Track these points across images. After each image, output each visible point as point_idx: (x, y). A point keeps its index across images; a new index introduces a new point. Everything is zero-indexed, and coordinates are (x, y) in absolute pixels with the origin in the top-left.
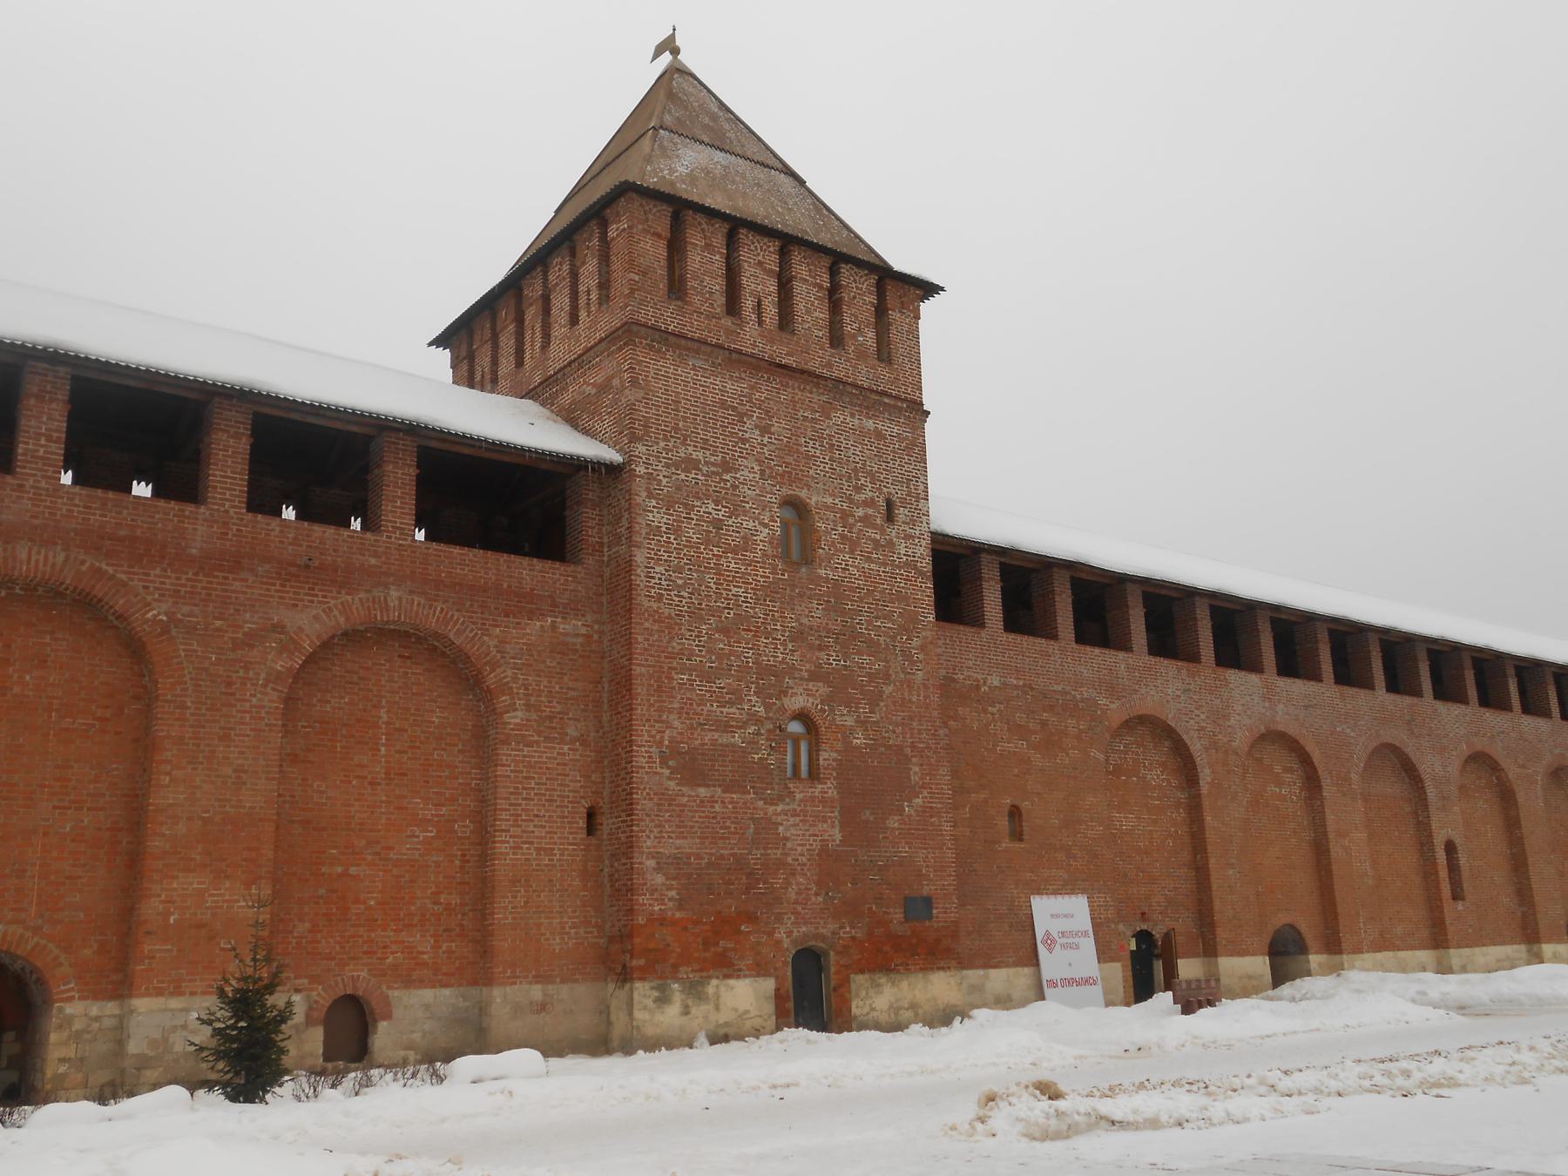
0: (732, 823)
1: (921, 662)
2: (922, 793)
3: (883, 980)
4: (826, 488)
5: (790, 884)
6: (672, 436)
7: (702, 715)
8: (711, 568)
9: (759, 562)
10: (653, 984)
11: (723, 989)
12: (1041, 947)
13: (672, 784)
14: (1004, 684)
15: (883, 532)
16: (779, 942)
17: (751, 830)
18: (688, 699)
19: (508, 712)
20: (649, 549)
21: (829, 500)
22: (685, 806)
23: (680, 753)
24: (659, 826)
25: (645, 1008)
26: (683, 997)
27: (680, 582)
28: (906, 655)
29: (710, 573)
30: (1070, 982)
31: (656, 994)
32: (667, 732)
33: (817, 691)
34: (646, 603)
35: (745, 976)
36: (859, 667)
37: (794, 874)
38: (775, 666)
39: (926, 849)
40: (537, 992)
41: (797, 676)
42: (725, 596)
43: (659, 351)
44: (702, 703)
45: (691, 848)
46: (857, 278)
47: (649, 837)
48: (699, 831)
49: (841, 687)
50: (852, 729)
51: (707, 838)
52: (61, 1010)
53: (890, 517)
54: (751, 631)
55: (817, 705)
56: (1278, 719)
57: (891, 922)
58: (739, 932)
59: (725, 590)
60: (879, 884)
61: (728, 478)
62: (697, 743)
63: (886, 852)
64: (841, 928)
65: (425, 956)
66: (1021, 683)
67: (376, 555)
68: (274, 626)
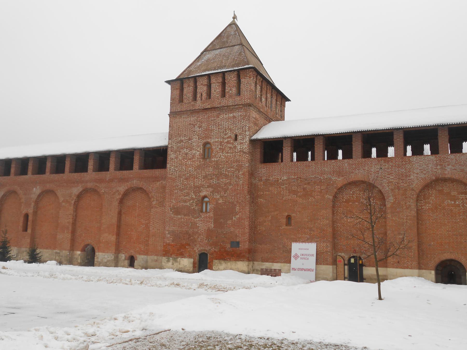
0: (186, 223)
1: (242, 178)
2: (239, 214)
3: (223, 262)
4: (216, 137)
5: (199, 237)
6: (177, 136)
7: (180, 199)
8: (184, 165)
9: (196, 161)
10: (167, 258)
11: (181, 260)
12: (292, 258)
13: (172, 215)
14: (289, 178)
15: (233, 144)
16: (195, 251)
17: (190, 225)
18: (177, 196)
19: (153, 202)
20: (170, 163)
21: (217, 140)
22: (175, 220)
23: (174, 208)
24: (170, 224)
25: (164, 262)
26: (173, 261)
27: (177, 170)
28: (238, 177)
29: (184, 166)
30: (302, 269)
31: (167, 260)
32: (172, 204)
33: (209, 190)
34: (169, 176)
35: (186, 258)
36: (222, 182)
37: (200, 235)
38: (198, 185)
39: (239, 229)
40: (156, 258)
41: (204, 187)
42: (187, 171)
43: (175, 117)
44: (180, 196)
45: (176, 229)
46: (230, 75)
47: (167, 227)
48: (178, 225)
49: (216, 189)
50: (219, 199)
51: (180, 227)
52: (96, 254)
53: (236, 139)
54: (193, 178)
55: (209, 194)
56: (446, 172)
57: (226, 248)
58: (185, 248)
59: (187, 169)
60: (224, 238)
61: (190, 142)
62: (178, 205)
63: (226, 230)
64: (211, 248)
65: (142, 249)
66: (296, 177)
67: (132, 174)
68: (117, 191)
